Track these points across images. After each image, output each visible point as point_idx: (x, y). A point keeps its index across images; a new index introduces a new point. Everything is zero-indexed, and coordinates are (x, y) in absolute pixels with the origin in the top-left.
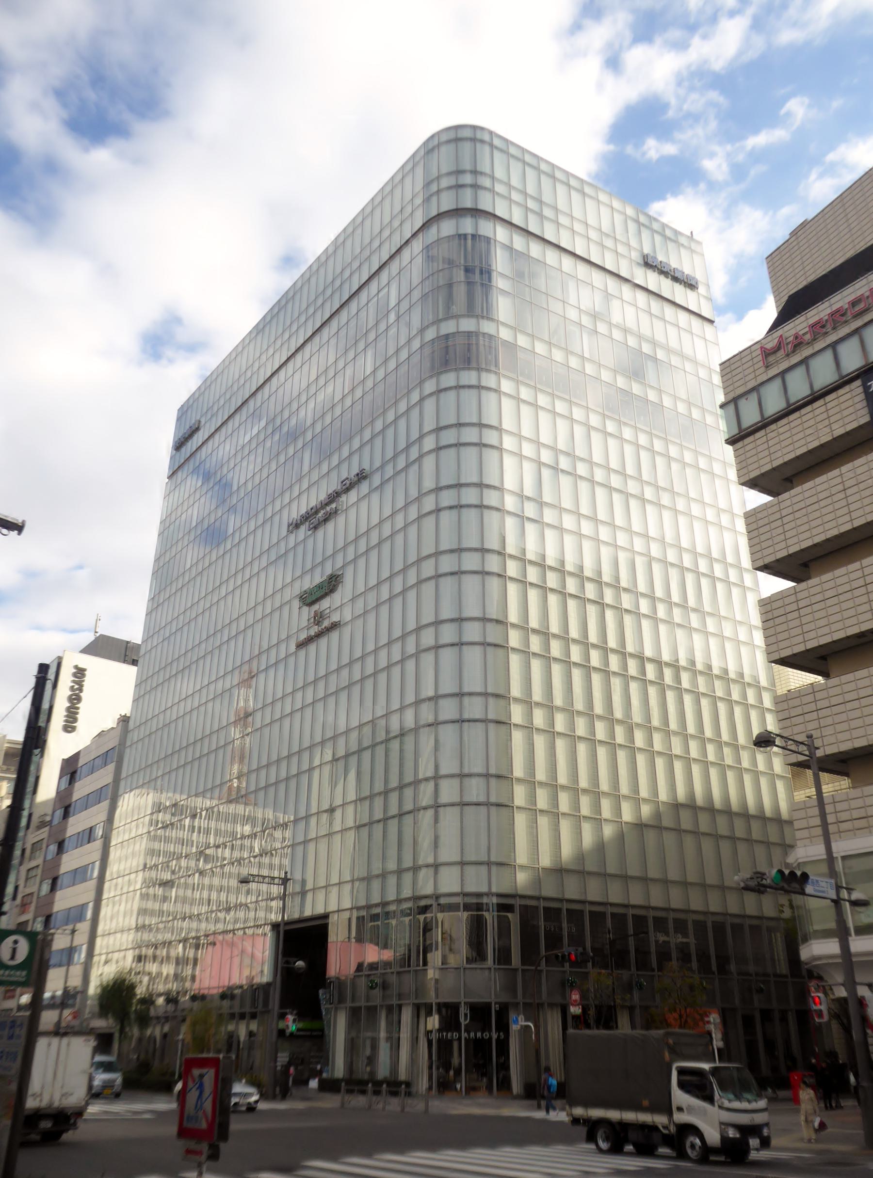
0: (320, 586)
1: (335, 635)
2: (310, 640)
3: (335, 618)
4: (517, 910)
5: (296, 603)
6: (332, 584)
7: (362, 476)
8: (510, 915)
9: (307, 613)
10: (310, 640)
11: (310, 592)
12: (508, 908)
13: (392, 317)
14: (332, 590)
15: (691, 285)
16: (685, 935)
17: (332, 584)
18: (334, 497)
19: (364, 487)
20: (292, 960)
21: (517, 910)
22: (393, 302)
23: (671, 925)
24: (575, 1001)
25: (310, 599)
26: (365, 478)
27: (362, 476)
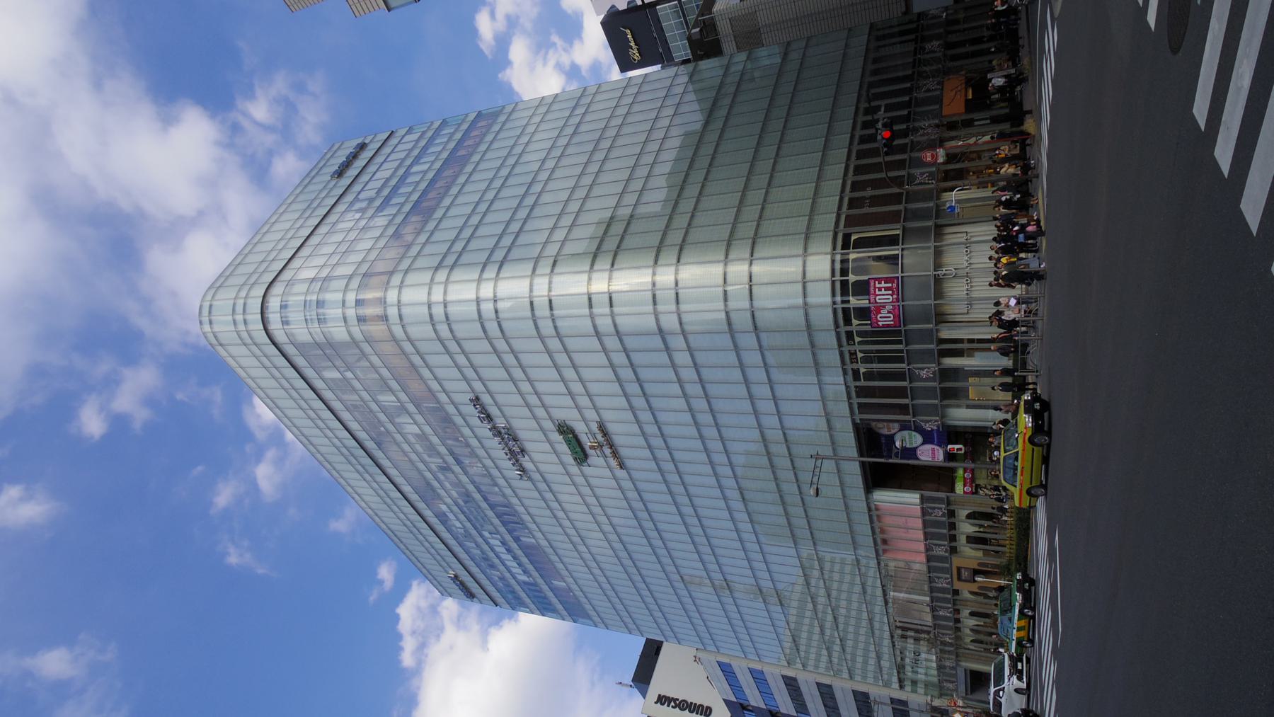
0: (568, 443)
1: (611, 428)
2: (615, 454)
3: (594, 427)
4: (849, 230)
5: (586, 470)
6: (565, 430)
7: (476, 401)
8: (853, 238)
9: (595, 458)
10: (615, 454)
11: (573, 452)
12: (847, 237)
13: (349, 375)
14: (572, 432)
15: (362, 147)
16: (878, 108)
17: (565, 430)
18: (497, 432)
19: (486, 399)
20: (895, 451)
21: (849, 230)
22: (336, 375)
23: (869, 118)
24: (932, 156)
25: (581, 455)
26: (477, 398)
27: (476, 401)
